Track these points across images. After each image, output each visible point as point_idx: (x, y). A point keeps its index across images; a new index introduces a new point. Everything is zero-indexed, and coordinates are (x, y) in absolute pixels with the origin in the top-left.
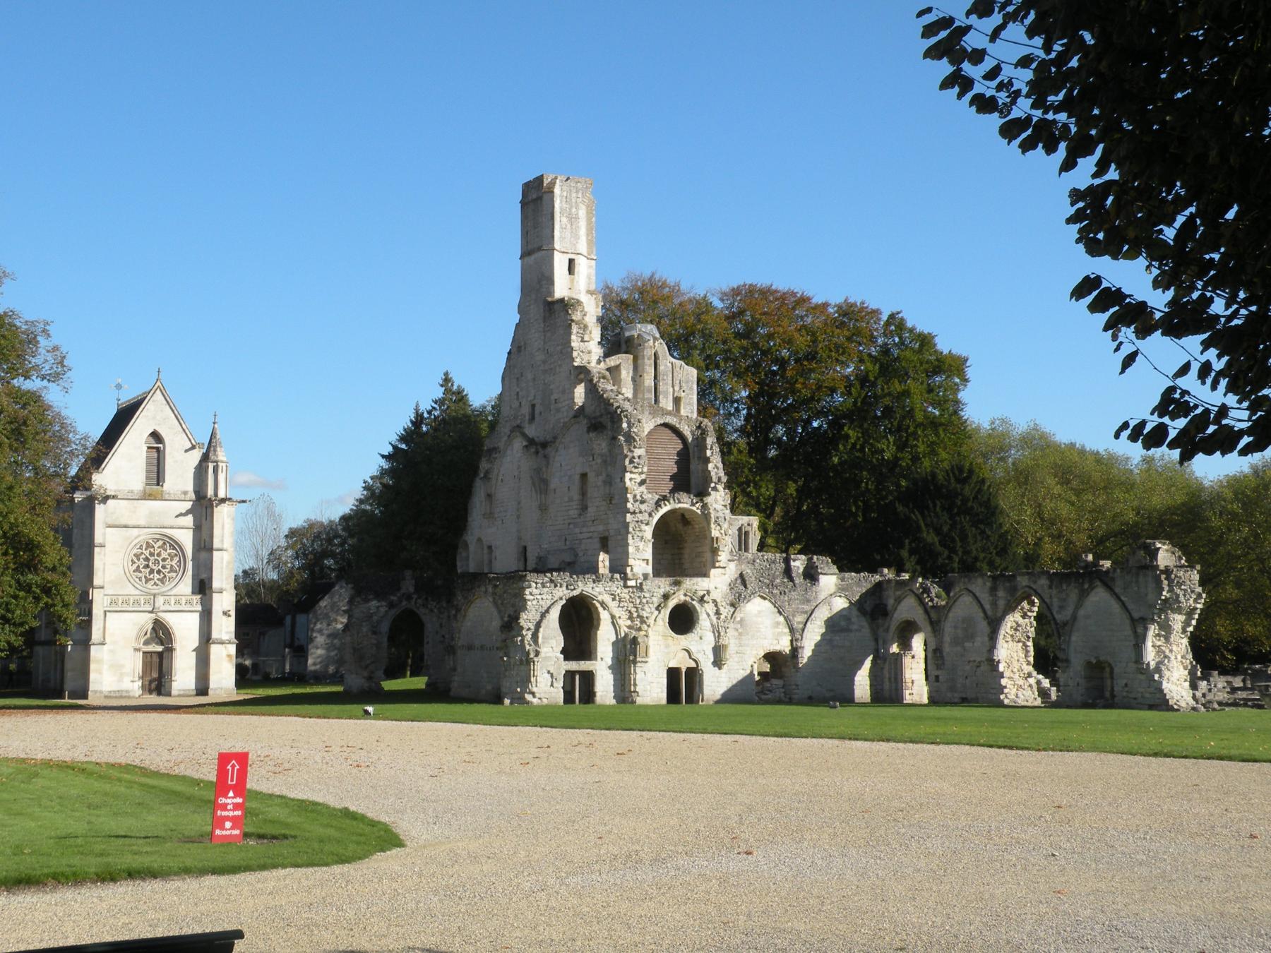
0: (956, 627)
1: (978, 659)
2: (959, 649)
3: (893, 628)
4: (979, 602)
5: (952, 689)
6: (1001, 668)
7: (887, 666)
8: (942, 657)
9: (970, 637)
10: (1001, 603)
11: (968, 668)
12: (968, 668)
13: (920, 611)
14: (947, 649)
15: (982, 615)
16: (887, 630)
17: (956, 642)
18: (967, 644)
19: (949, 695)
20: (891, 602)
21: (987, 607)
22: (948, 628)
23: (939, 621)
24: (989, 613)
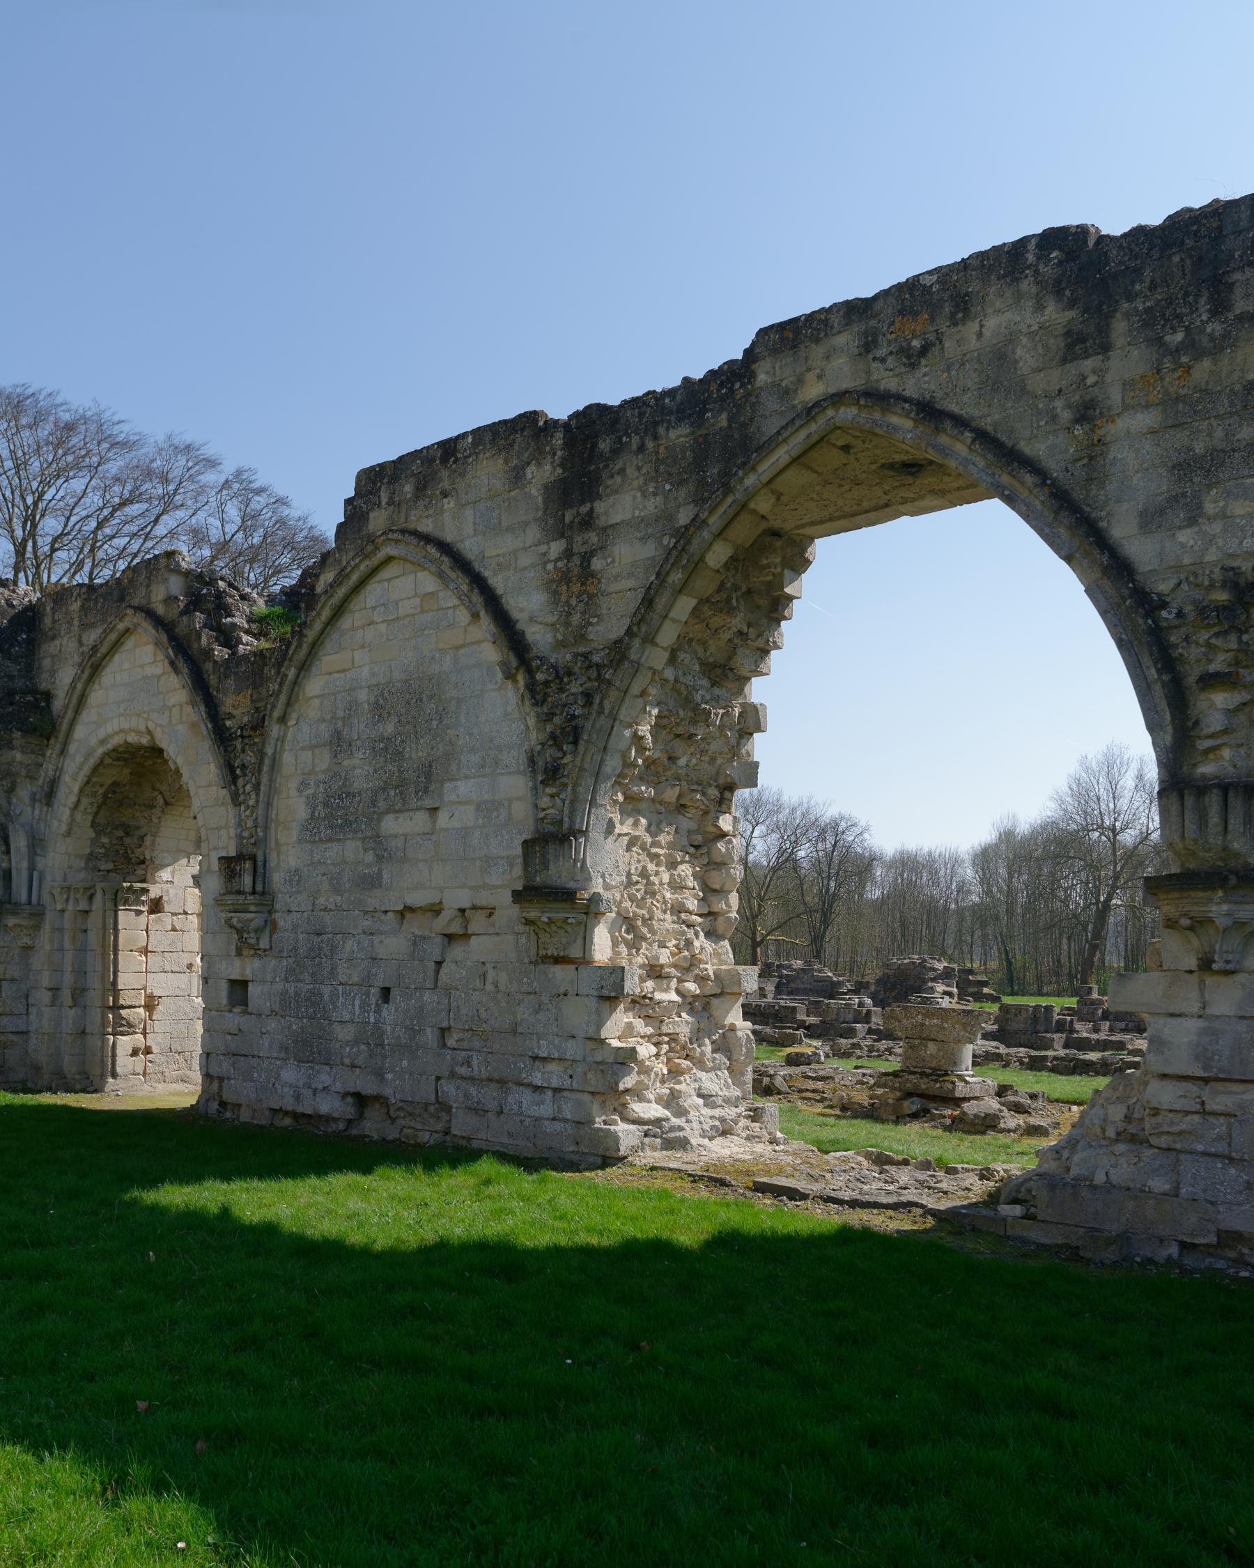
0: (338, 743)
1: (458, 898)
2: (351, 848)
3: (70, 787)
4: (479, 582)
5: (310, 1049)
6: (602, 946)
7: (45, 941)
8: (264, 895)
9: (418, 784)
10: (626, 561)
11: (394, 945)
12: (394, 945)
13: (176, 691)
14: (288, 855)
15: (491, 653)
16: (49, 796)
17: (338, 813)
18: (391, 825)
19: (290, 1074)
20: (63, 679)
21: (529, 604)
22: (299, 754)
23: (259, 725)
24: (539, 636)
